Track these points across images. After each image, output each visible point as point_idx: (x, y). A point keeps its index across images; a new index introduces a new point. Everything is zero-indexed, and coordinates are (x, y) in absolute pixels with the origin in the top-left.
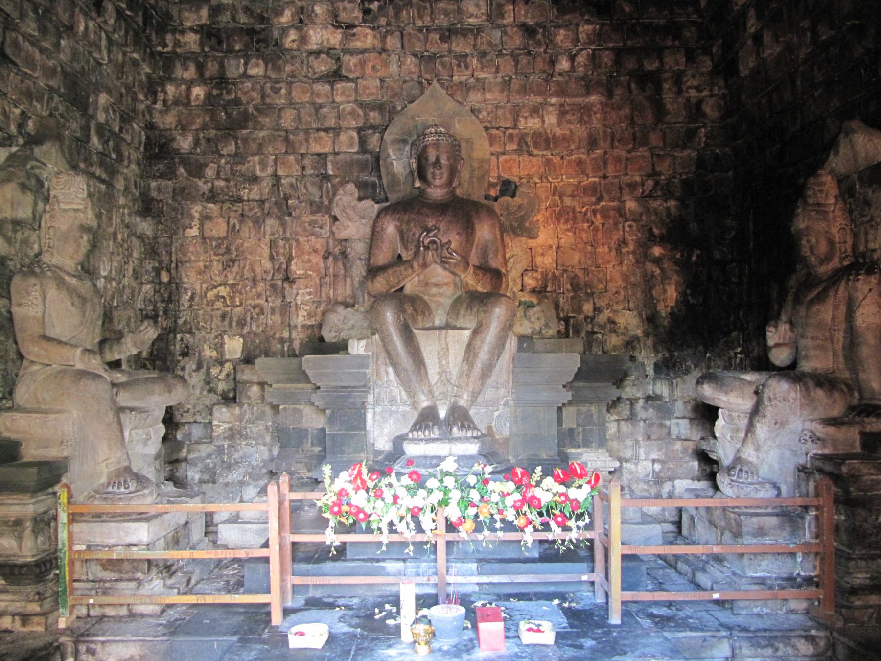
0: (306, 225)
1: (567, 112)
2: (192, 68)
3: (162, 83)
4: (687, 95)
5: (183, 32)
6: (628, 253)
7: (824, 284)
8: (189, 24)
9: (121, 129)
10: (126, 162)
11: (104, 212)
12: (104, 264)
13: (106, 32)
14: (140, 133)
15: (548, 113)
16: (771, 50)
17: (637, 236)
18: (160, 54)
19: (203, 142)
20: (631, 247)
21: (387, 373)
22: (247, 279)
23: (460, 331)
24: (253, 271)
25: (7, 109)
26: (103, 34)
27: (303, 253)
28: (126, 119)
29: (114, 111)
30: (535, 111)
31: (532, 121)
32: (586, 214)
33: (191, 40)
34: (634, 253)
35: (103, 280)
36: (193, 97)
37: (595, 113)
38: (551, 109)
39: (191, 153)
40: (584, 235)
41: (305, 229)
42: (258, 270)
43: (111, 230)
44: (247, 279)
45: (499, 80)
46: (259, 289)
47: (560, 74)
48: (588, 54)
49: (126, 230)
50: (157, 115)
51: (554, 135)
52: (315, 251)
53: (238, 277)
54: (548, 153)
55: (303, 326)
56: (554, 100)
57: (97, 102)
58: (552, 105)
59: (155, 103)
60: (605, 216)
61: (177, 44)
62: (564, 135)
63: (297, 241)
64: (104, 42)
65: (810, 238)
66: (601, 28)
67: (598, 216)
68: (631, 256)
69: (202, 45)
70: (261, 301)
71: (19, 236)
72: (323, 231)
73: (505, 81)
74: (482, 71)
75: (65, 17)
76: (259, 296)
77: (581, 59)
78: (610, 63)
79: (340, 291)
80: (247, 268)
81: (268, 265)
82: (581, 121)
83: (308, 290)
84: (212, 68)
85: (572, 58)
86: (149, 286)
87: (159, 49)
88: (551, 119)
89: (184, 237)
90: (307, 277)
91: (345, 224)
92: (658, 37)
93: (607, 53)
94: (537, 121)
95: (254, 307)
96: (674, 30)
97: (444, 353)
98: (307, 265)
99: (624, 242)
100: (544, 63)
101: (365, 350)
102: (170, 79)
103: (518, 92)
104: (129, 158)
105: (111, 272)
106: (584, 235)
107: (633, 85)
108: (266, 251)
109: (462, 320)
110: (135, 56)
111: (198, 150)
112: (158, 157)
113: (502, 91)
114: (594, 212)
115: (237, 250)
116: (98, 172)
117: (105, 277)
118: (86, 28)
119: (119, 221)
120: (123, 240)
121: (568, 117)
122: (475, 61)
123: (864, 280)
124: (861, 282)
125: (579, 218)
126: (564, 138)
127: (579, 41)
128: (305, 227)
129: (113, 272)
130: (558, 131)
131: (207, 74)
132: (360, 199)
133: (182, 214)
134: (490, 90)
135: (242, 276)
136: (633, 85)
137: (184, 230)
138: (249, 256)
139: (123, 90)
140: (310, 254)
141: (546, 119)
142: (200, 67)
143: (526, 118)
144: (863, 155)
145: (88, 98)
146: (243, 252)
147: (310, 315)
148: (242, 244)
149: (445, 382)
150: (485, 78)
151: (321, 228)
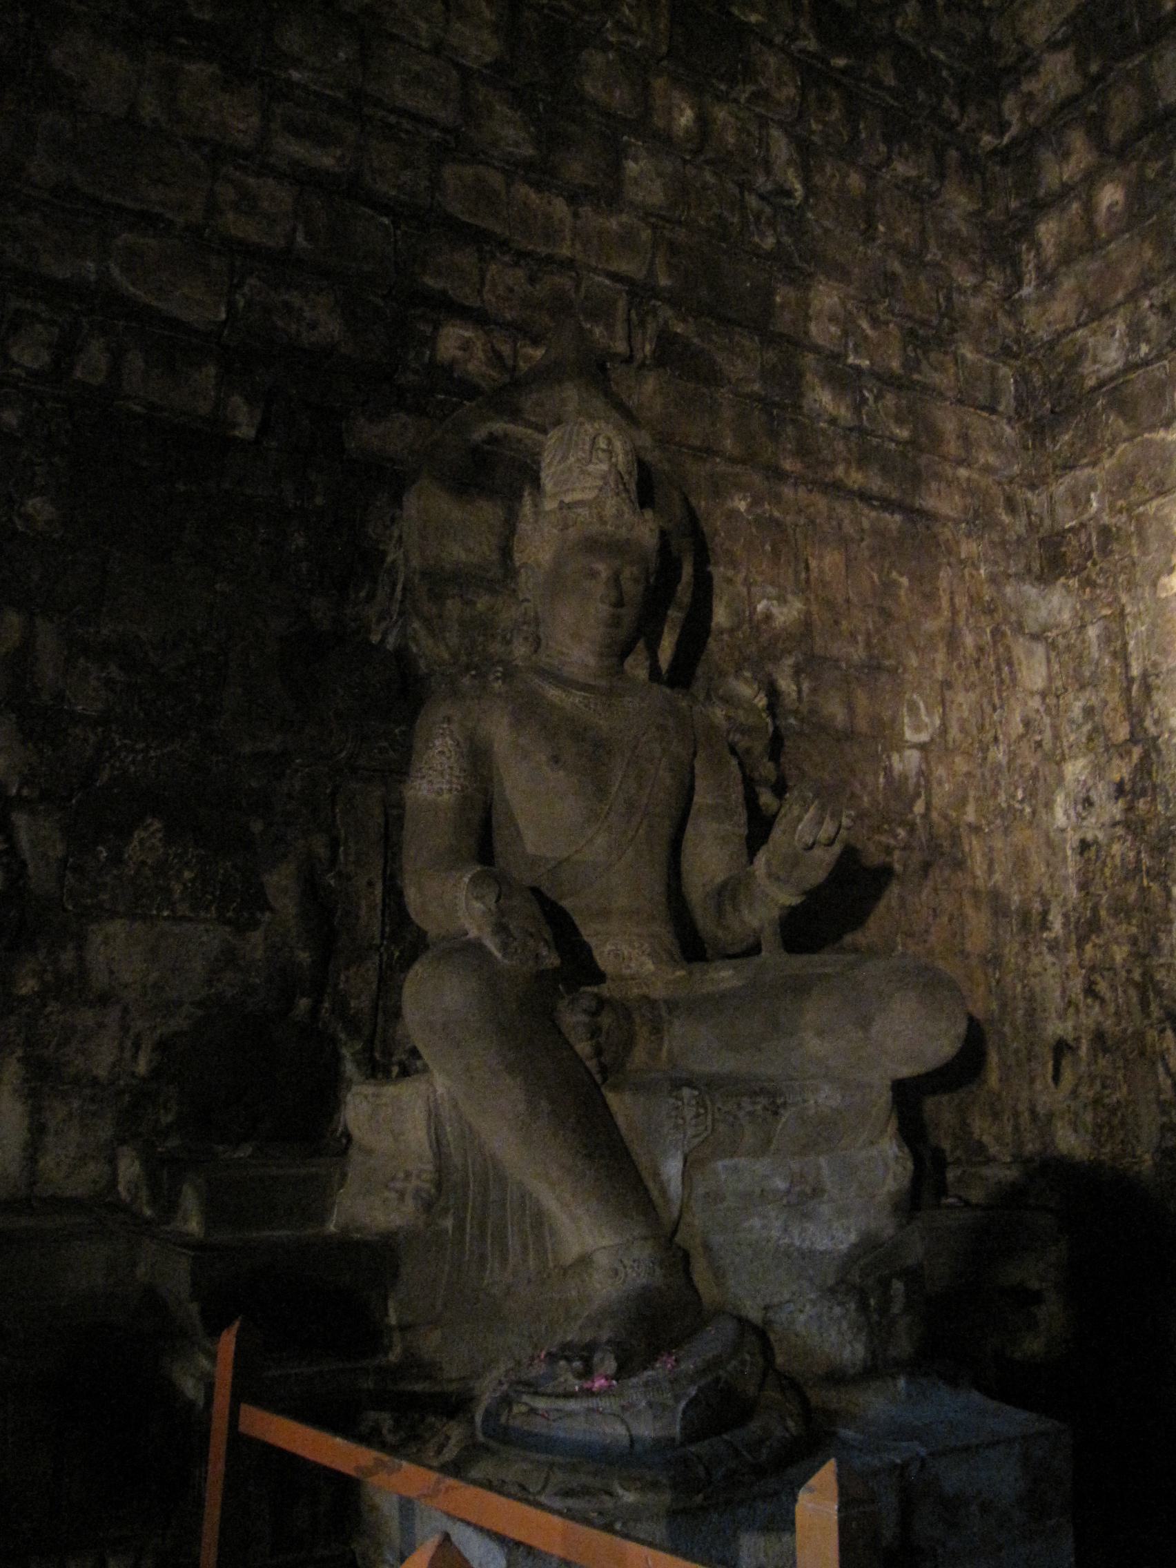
2: (1077, 139)
3: (1026, 231)
5: (1033, 71)
8: (1040, 35)
9: (911, 365)
10: (953, 447)
11: (904, 581)
12: (913, 709)
13: (780, 124)
14: (993, 371)
18: (994, 152)
19: (1152, 321)
25: (506, 349)
26: (775, 133)
28: (927, 338)
29: (875, 322)
33: (1057, 76)
35: (914, 756)
36: (1101, 217)
39: (1130, 367)
43: (932, 625)
49: (984, 620)
50: (1030, 313)
57: (805, 304)
59: (1019, 282)
61: (1029, 102)
64: (781, 148)
69: (1081, 63)
71: (453, 607)
75: (620, 98)
84: (1124, 107)
86: (1081, 762)
87: (987, 140)
89: (1157, 600)
102: (1040, 207)
104: (964, 438)
105: (944, 730)
110: (901, 168)
111: (1144, 349)
112: (1059, 417)
116: (856, 479)
117: (922, 747)
118: (703, 120)
119: (961, 601)
120: (981, 649)
129: (954, 732)
131: (1115, 135)
133: (1143, 542)
137: (1154, 585)
139: (896, 266)
142: (1096, 127)
145: (770, 293)
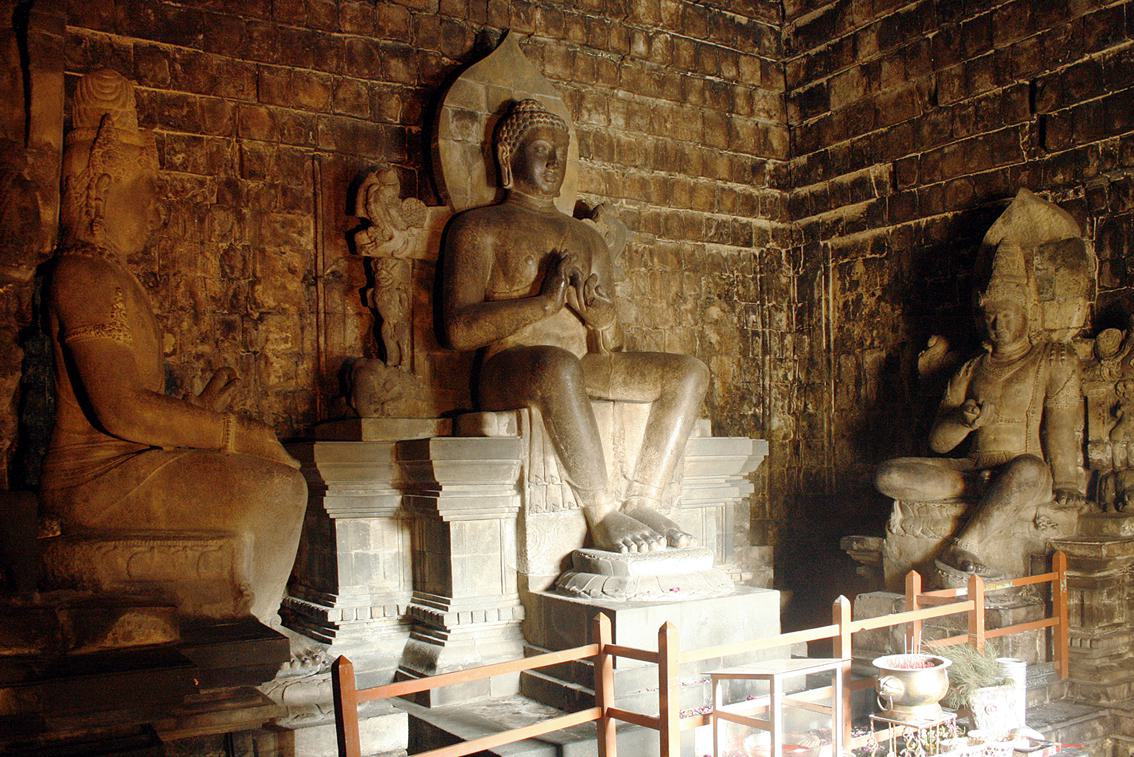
0: (278, 226)
1: (635, 113)
4: (756, 119)
6: (686, 310)
7: (1020, 364)
15: (616, 110)
16: (891, 87)
17: (695, 291)
20: (689, 306)
21: (545, 462)
22: (182, 308)
23: (638, 405)
24: (193, 295)
27: (273, 272)
30: (602, 104)
31: (596, 117)
32: (642, 256)
34: (692, 312)
37: (666, 122)
38: (617, 104)
40: (642, 284)
41: (275, 233)
42: (201, 295)
44: (182, 308)
45: (562, 49)
46: (204, 327)
47: (633, 60)
48: (666, 41)
51: (619, 141)
52: (293, 271)
53: (167, 305)
54: (609, 167)
55: (277, 394)
56: (621, 94)
58: (619, 100)
60: (663, 261)
62: (630, 143)
63: (263, 252)
65: (1008, 312)
66: (684, 10)
67: (656, 260)
68: (689, 316)
70: (205, 348)
72: (303, 240)
73: (568, 52)
74: (547, 32)
76: (204, 339)
77: (658, 44)
78: (688, 59)
79: (336, 339)
80: (182, 289)
81: (216, 287)
82: (652, 132)
83: (284, 335)
85: (649, 41)
88: (619, 120)
90: (283, 312)
91: (387, 233)
92: (739, 38)
93: (686, 44)
94: (603, 117)
95: (199, 357)
96: (752, 33)
97: (620, 437)
98: (280, 294)
99: (680, 297)
100: (619, 39)
101: (508, 431)
103: (585, 74)
106: (642, 284)
107: (707, 94)
108: (214, 264)
109: (618, 390)
113: (566, 66)
114: (651, 253)
115: (164, 255)
121: (637, 120)
122: (538, 15)
123: (1068, 360)
124: (1065, 363)
125: (635, 258)
126: (631, 148)
127: (661, 21)
128: (274, 230)
130: (624, 138)
132: (403, 197)
134: (549, 62)
135: (174, 302)
136: (707, 94)
138: (184, 270)
140: (283, 275)
141: (612, 116)
143: (589, 111)
144: (1046, 228)
146: (174, 261)
147: (287, 377)
148: (172, 247)
149: (620, 475)
150: (545, 43)
151: (300, 233)
